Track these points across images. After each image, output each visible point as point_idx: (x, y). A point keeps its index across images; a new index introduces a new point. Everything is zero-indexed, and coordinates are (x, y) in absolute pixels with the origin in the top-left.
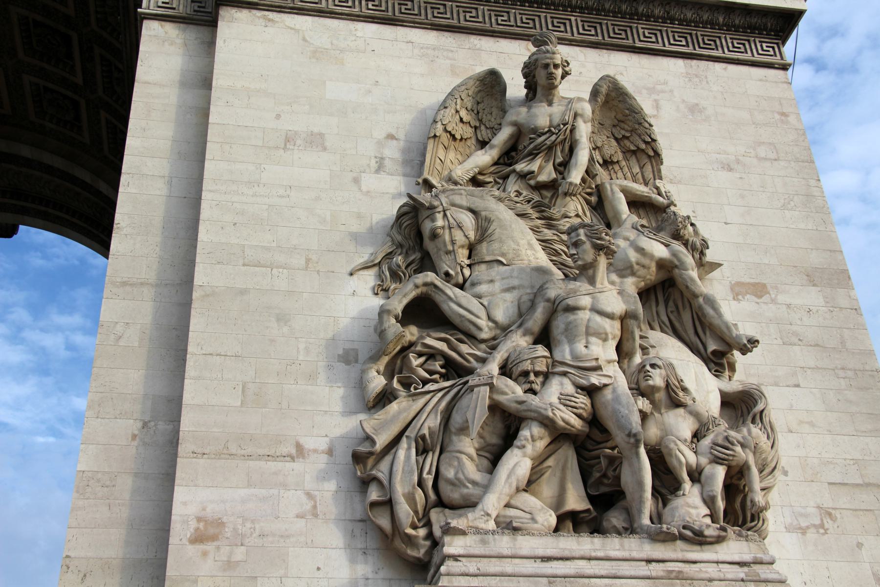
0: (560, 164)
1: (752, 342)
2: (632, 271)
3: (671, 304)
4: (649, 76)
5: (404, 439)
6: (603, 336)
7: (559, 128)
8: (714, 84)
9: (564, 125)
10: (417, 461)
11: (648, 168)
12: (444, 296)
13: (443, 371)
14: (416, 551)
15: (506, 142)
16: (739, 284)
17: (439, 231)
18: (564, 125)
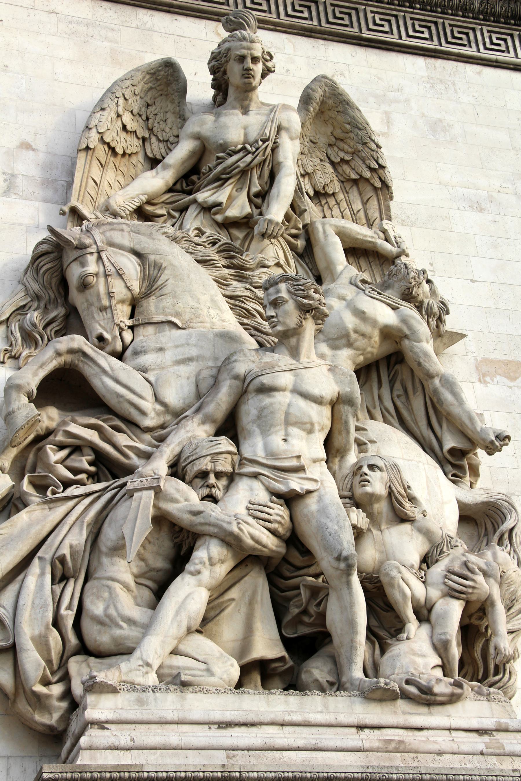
0: (257, 195)
1: (502, 439)
2: (349, 341)
3: (398, 385)
4: (379, 78)
5: (36, 561)
6: (308, 426)
7: (257, 146)
8: (464, 93)
9: (264, 141)
10: (53, 592)
11: (374, 204)
12: (96, 368)
13: (92, 469)
14: (47, 716)
15: (184, 162)
16: (487, 361)
17: (91, 279)
18: (264, 141)
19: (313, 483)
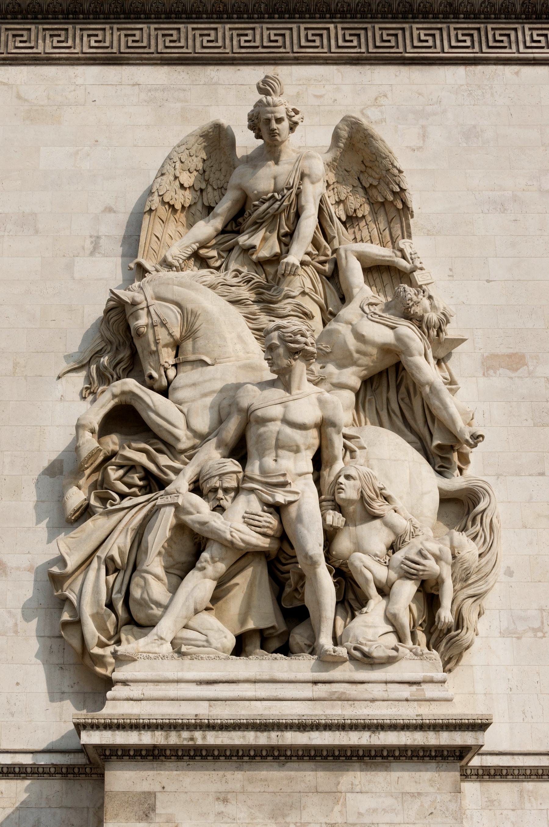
0: (286, 235)
1: (476, 438)
2: (352, 359)
3: (403, 389)
4: (420, 94)
6: (295, 448)
7: (283, 194)
8: (500, 96)
9: (289, 189)
10: (107, 582)
12: (143, 404)
13: (141, 483)
14: (105, 669)
15: (230, 209)
16: (494, 356)
17: (142, 329)
18: (289, 189)
19: (296, 495)
